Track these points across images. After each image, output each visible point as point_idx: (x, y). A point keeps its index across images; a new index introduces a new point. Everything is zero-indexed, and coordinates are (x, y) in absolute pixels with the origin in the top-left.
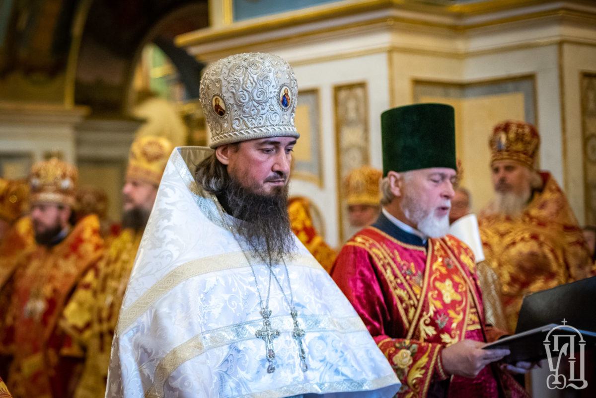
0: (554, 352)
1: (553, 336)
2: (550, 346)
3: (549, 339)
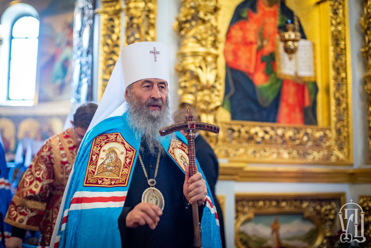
0: (345, 219)
1: (345, 209)
2: (342, 215)
3: (342, 211)
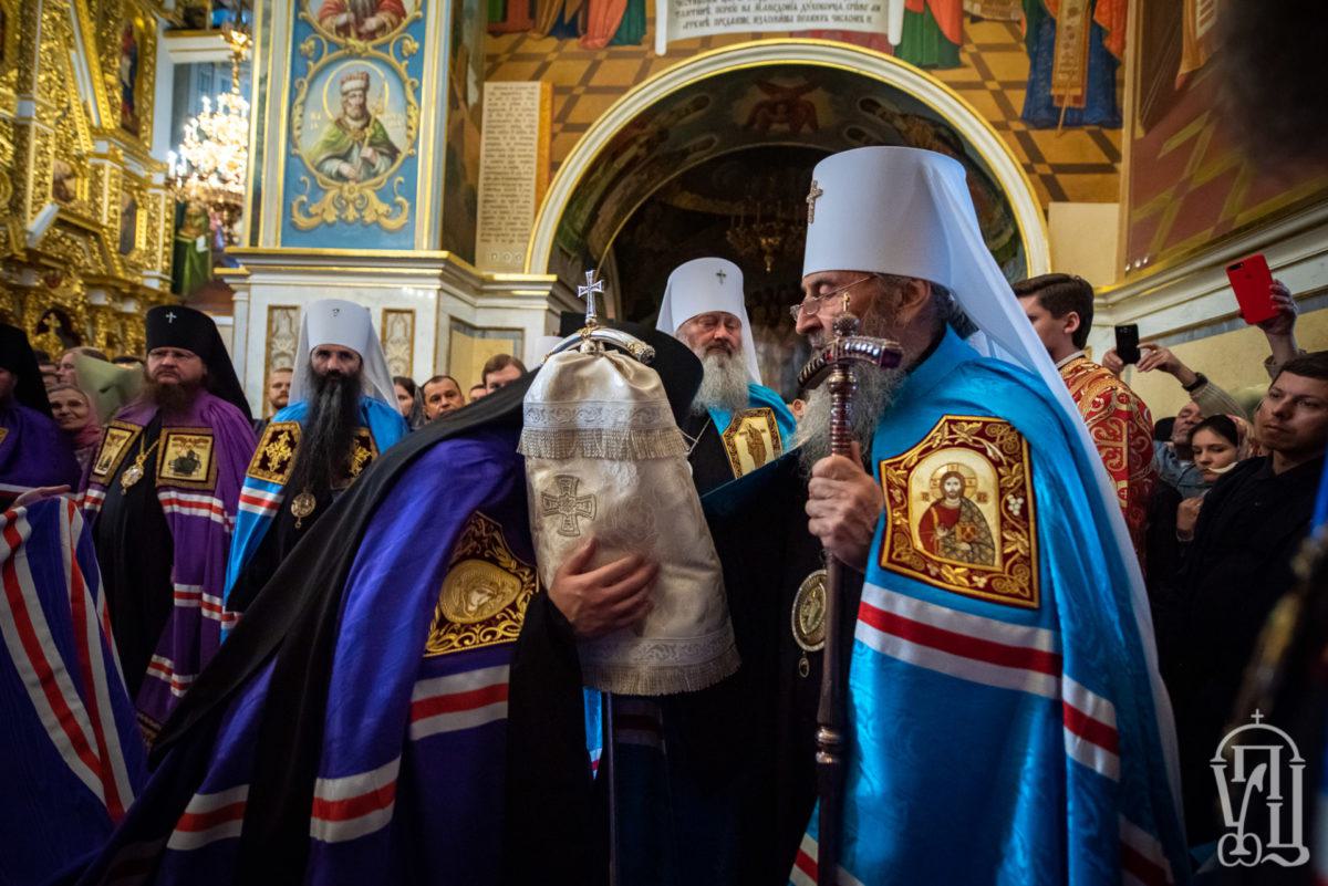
1: (1233, 747)
3: (1223, 755)
